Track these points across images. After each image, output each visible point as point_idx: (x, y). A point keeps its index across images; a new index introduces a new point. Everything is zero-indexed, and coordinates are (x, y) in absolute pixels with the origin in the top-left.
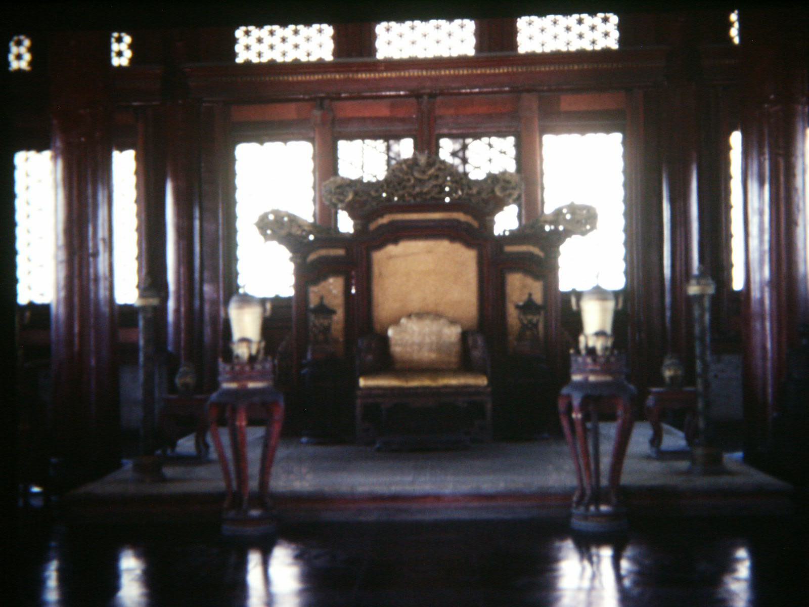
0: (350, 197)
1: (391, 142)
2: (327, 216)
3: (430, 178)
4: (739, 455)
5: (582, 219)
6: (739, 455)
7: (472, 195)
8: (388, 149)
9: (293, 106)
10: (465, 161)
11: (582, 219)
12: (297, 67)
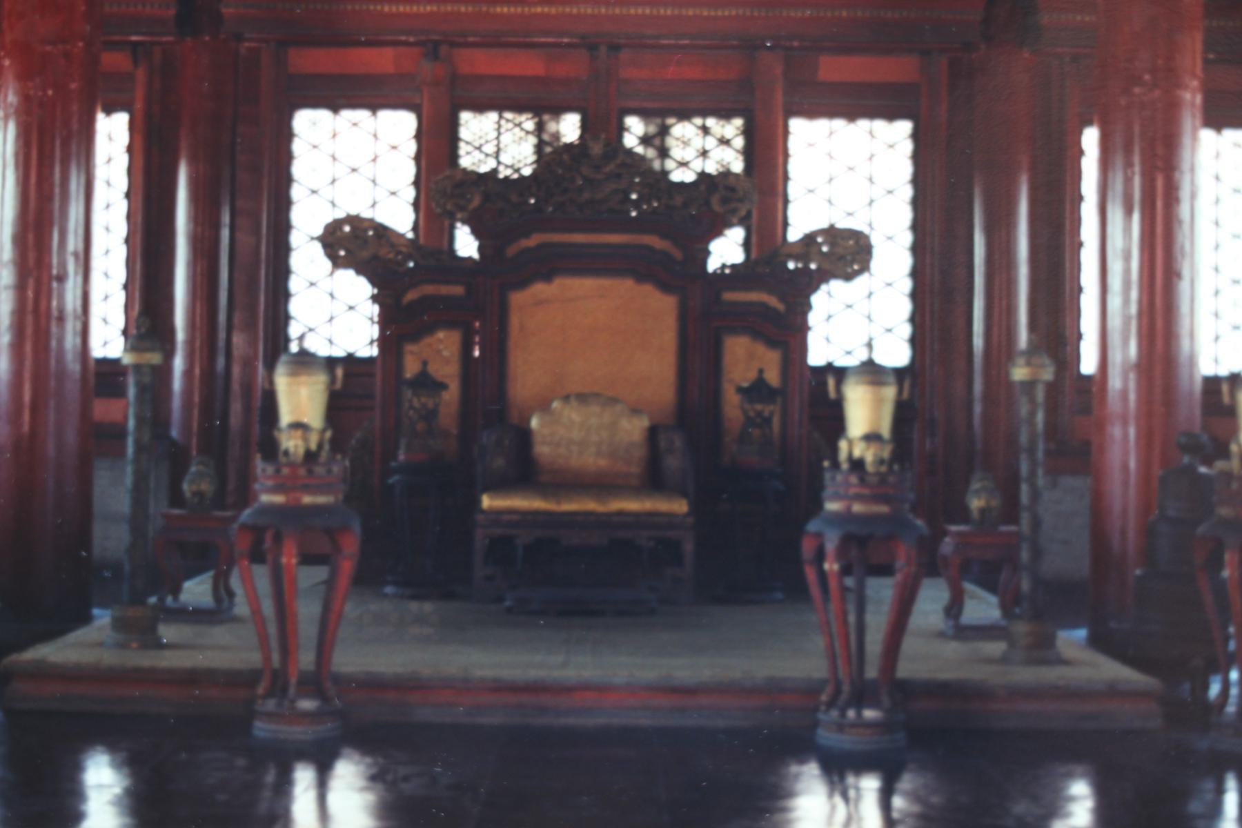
0: (476, 201)
1: (546, 117)
4: (1081, 633)
5: (846, 253)
6: (1081, 633)
8: (540, 128)
9: (389, 52)
10: (664, 153)
11: (846, 253)
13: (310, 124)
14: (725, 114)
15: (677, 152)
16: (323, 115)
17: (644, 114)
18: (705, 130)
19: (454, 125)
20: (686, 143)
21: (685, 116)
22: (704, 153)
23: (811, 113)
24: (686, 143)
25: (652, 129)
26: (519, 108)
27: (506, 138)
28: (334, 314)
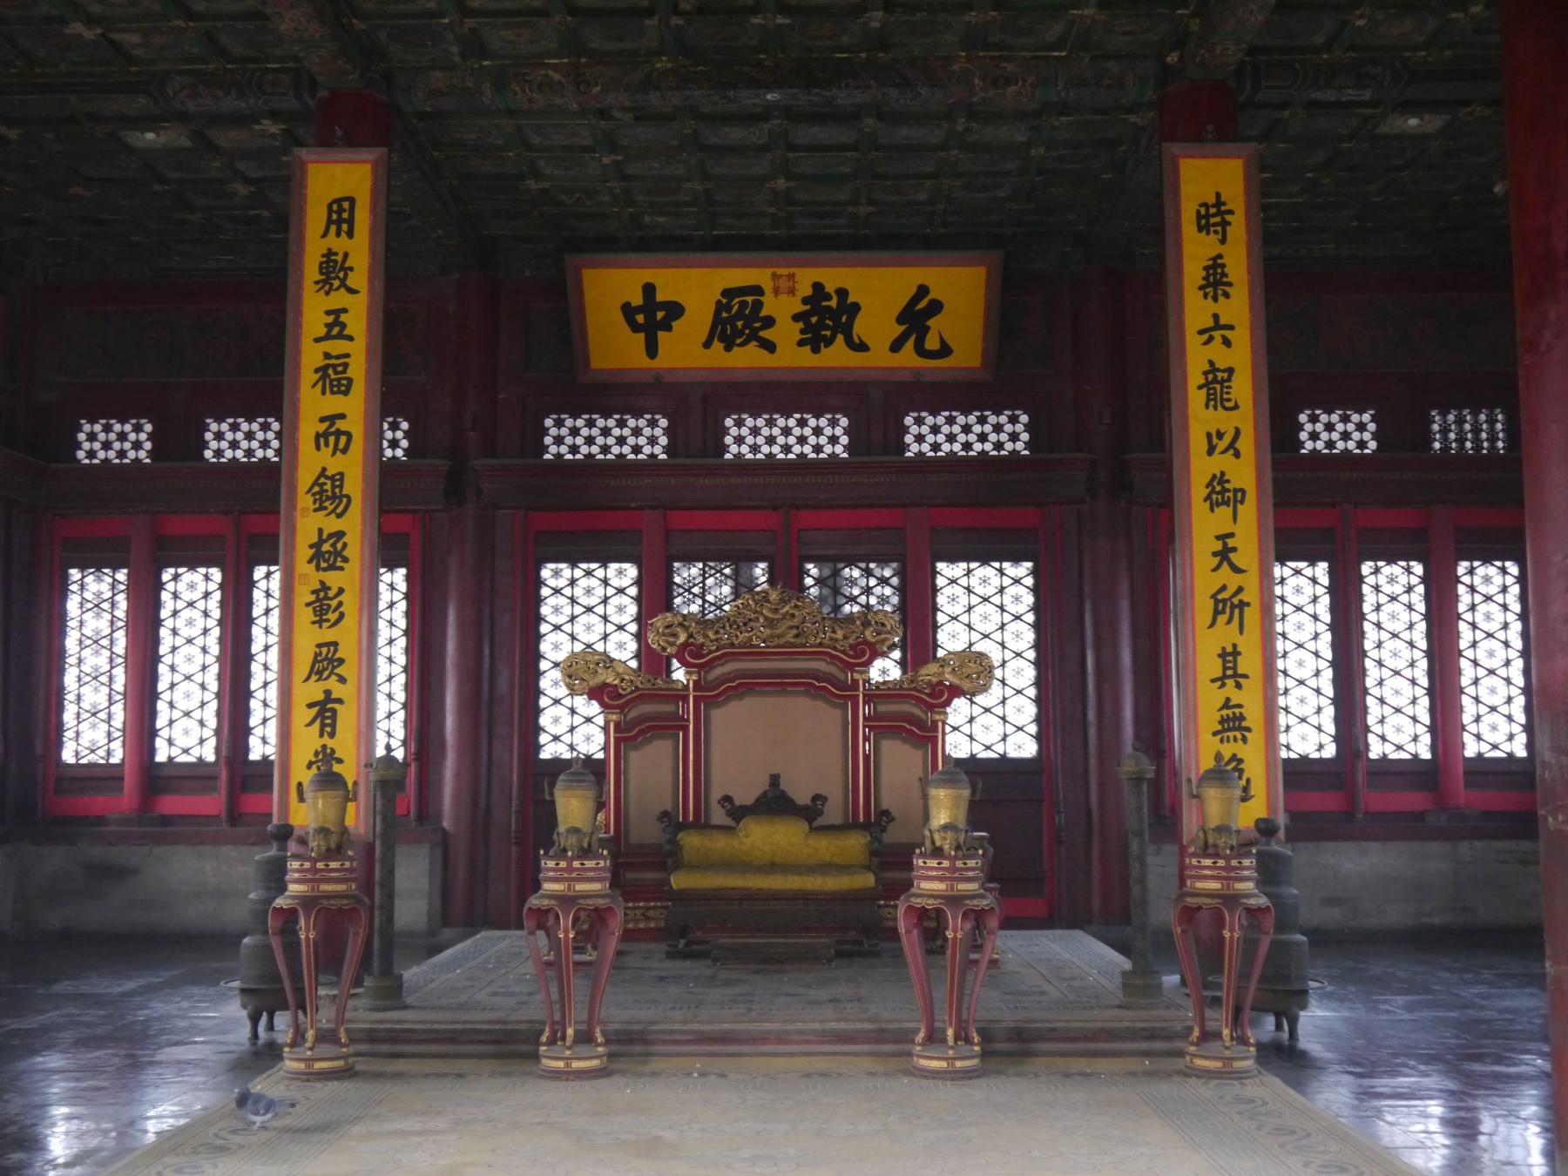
0: (682, 638)
3: (784, 618)
4: (1176, 978)
5: (975, 672)
6: (1176, 978)
8: (736, 576)
10: (836, 591)
11: (975, 672)
13: (553, 575)
14: (883, 561)
15: (847, 591)
18: (868, 573)
19: (669, 573)
20: (853, 582)
21: (851, 563)
22: (868, 591)
23: (952, 559)
25: (827, 572)
26: (720, 559)
27: (710, 581)
28: (571, 727)
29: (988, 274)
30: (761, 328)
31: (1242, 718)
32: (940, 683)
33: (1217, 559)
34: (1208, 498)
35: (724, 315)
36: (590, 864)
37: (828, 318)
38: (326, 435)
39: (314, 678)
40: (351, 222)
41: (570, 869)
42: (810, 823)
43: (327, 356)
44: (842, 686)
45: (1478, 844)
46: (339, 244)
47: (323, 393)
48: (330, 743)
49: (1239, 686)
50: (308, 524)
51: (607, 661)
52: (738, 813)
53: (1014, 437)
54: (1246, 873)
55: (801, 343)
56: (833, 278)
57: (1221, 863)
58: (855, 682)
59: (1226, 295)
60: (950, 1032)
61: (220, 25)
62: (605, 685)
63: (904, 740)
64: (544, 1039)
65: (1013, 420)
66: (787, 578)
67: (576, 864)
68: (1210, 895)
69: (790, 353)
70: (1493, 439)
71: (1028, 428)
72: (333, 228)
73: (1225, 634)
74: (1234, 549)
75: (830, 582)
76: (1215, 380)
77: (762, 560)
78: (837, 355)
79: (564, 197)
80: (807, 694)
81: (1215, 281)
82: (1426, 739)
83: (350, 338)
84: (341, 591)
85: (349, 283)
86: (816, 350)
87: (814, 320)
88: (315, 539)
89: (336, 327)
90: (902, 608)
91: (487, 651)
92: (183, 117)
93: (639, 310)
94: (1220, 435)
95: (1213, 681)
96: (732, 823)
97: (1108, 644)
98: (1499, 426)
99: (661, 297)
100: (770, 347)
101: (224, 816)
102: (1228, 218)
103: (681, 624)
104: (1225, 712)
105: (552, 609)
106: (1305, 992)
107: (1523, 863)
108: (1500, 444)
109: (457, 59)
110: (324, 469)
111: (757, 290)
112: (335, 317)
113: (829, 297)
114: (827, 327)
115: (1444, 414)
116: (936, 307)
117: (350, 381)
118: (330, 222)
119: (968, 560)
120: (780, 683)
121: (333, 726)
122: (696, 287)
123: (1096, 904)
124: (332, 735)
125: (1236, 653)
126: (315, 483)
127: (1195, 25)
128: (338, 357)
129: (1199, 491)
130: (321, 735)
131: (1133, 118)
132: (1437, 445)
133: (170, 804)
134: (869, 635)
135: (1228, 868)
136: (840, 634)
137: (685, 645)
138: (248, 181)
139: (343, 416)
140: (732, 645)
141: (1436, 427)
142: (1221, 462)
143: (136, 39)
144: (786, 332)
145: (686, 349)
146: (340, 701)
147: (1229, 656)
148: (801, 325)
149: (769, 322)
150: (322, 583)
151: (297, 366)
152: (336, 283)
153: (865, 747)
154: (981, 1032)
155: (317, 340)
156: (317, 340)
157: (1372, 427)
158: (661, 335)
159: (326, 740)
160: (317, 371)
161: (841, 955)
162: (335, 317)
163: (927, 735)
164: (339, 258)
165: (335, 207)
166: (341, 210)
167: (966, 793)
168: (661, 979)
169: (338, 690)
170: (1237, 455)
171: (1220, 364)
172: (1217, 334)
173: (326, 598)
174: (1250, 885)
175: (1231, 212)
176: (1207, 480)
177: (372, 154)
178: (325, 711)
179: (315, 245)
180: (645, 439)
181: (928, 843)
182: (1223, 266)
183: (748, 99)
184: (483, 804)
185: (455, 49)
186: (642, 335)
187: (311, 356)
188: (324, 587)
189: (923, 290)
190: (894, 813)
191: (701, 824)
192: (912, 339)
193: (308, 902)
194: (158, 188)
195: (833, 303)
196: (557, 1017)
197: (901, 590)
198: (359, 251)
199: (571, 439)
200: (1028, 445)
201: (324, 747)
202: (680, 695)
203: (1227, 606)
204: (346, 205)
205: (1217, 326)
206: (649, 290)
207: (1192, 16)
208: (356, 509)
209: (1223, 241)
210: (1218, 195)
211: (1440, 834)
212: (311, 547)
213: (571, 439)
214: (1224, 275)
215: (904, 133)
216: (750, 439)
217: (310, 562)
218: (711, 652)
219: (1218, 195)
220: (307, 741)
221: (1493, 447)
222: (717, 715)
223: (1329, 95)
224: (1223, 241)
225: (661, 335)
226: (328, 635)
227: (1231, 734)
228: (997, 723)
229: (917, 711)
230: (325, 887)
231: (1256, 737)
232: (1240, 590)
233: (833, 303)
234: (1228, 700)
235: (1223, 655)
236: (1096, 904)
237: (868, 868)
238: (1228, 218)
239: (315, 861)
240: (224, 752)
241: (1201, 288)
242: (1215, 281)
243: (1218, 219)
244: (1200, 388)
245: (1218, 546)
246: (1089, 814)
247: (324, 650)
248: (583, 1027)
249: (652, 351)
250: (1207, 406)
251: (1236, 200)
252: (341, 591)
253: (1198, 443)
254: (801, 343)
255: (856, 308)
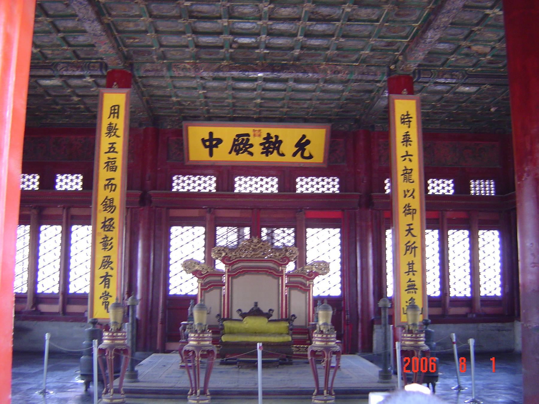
0: (224, 254)
2: (210, 261)
5: (323, 268)
7: (276, 256)
8: (239, 231)
9: (197, 210)
10: (273, 238)
11: (323, 268)
12: (199, 194)
13: (175, 230)
14: (289, 227)
15: (277, 238)
16: (179, 228)
17: (267, 227)
20: (278, 235)
21: (278, 228)
23: (313, 227)
24: (278, 235)
25: (270, 231)
29: (326, 132)
30: (249, 148)
31: (414, 285)
32: (312, 271)
33: (407, 232)
34: (404, 212)
35: (236, 143)
36: (206, 335)
37: (271, 145)
38: (108, 185)
39: (103, 268)
40: (118, 113)
41: (199, 337)
42: (268, 318)
43: (109, 158)
44: (278, 271)
45: (485, 324)
46: (114, 121)
47: (107, 170)
48: (108, 290)
49: (414, 275)
50: (102, 215)
51: (199, 263)
52: (244, 315)
53: (334, 186)
54: (422, 339)
55: (262, 153)
56: (274, 131)
57: (414, 336)
58: (282, 271)
59: (410, 145)
60: (325, 392)
61: (79, 48)
62: (197, 271)
63: (299, 291)
64: (189, 393)
65: (333, 180)
66: (256, 233)
67: (201, 335)
68: (411, 346)
69: (258, 156)
70: (490, 190)
71: (339, 183)
72: (112, 115)
73: (409, 257)
74: (412, 229)
75: (271, 235)
76: (406, 173)
77: (248, 226)
78: (274, 158)
79: (184, 103)
80: (266, 274)
81: (407, 140)
82: (469, 290)
83: (116, 152)
84: (112, 239)
85: (117, 134)
86: (267, 155)
87: (267, 145)
88: (103, 221)
89: (112, 149)
90: (295, 244)
91: (152, 257)
92: (61, 76)
93: (207, 141)
94: (408, 191)
95: (406, 273)
96: (240, 318)
97: (364, 257)
98: (492, 186)
99: (215, 137)
100: (251, 154)
101: (61, 313)
102: (411, 119)
103: (223, 250)
104: (409, 283)
105: (174, 243)
106: (437, 377)
107: (499, 330)
108: (492, 192)
109: (155, 60)
110: (107, 197)
111: (248, 135)
112: (112, 145)
113: (272, 138)
114: (271, 148)
115: (475, 181)
116: (308, 142)
117: (116, 167)
118: (111, 113)
119: (318, 227)
120: (257, 271)
121: (109, 284)
122: (227, 133)
123: (360, 346)
124: (108, 287)
125: (413, 264)
126: (104, 202)
127: (401, 58)
128: (113, 159)
129: (401, 210)
130: (105, 287)
131: (378, 85)
132: (472, 192)
133: (44, 308)
134: (287, 254)
135: (416, 337)
136: (277, 254)
137: (224, 257)
138: (78, 96)
139: (113, 179)
140: (241, 257)
141: (472, 186)
142: (408, 200)
143: (50, 52)
144: (257, 149)
145: (223, 154)
146: (111, 276)
147: (411, 264)
148: (262, 147)
149: (251, 146)
150: (106, 236)
151: (98, 161)
152: (113, 134)
153: (286, 292)
154: (335, 391)
155: (106, 153)
156: (106, 153)
157: (452, 185)
158: (215, 149)
159: (106, 289)
160: (106, 163)
161: (281, 364)
162: (112, 145)
163: (306, 289)
164: (114, 125)
165: (113, 108)
166: (115, 110)
167: (331, 313)
168: (221, 372)
169: (110, 272)
170: (414, 197)
171: (409, 168)
172: (407, 157)
173: (107, 241)
174: (423, 342)
175: (411, 118)
176: (404, 206)
177: (127, 90)
178: (106, 279)
179: (105, 121)
180: (208, 184)
181: (318, 329)
182: (409, 135)
183: (252, 75)
184: (150, 309)
185: (155, 57)
186: (208, 149)
187: (103, 158)
188: (106, 237)
189: (304, 136)
190: (297, 315)
191: (229, 319)
192: (300, 152)
193: (111, 347)
194: (48, 98)
195: (274, 140)
196: (194, 385)
197: (295, 238)
198: (120, 123)
199: (182, 184)
200: (339, 189)
201: (106, 291)
202: (220, 274)
203: (410, 248)
204: (116, 107)
205: (407, 155)
206: (211, 134)
207: (400, 55)
208: (117, 211)
209: (409, 127)
210: (408, 112)
211: (473, 321)
212: (103, 223)
213: (182, 184)
214: (410, 138)
215: (303, 86)
216: (244, 185)
217: (102, 228)
218: (233, 260)
219: (408, 112)
220: (100, 289)
221: (490, 193)
222: (235, 281)
223: (442, 81)
224: (409, 127)
225: (215, 149)
226: (107, 253)
227: (411, 290)
228: (329, 285)
229: (303, 281)
230: (116, 342)
231: (419, 292)
232: (414, 243)
233: (274, 140)
234: (410, 279)
235: (409, 264)
236: (360, 346)
237: (288, 334)
238: (411, 119)
239: (113, 333)
240: (61, 290)
241: (402, 142)
242: (407, 140)
243: (407, 120)
244: (402, 175)
245: (407, 228)
246: (358, 315)
247: (106, 258)
248: (203, 389)
249: (211, 154)
250: (404, 181)
251: (413, 114)
252: (112, 239)
253: (401, 194)
254: (262, 153)
255: (281, 142)
